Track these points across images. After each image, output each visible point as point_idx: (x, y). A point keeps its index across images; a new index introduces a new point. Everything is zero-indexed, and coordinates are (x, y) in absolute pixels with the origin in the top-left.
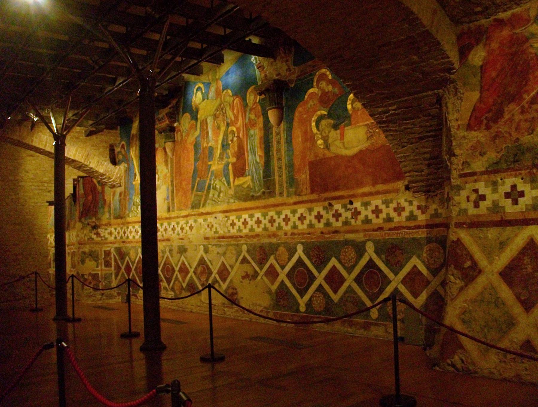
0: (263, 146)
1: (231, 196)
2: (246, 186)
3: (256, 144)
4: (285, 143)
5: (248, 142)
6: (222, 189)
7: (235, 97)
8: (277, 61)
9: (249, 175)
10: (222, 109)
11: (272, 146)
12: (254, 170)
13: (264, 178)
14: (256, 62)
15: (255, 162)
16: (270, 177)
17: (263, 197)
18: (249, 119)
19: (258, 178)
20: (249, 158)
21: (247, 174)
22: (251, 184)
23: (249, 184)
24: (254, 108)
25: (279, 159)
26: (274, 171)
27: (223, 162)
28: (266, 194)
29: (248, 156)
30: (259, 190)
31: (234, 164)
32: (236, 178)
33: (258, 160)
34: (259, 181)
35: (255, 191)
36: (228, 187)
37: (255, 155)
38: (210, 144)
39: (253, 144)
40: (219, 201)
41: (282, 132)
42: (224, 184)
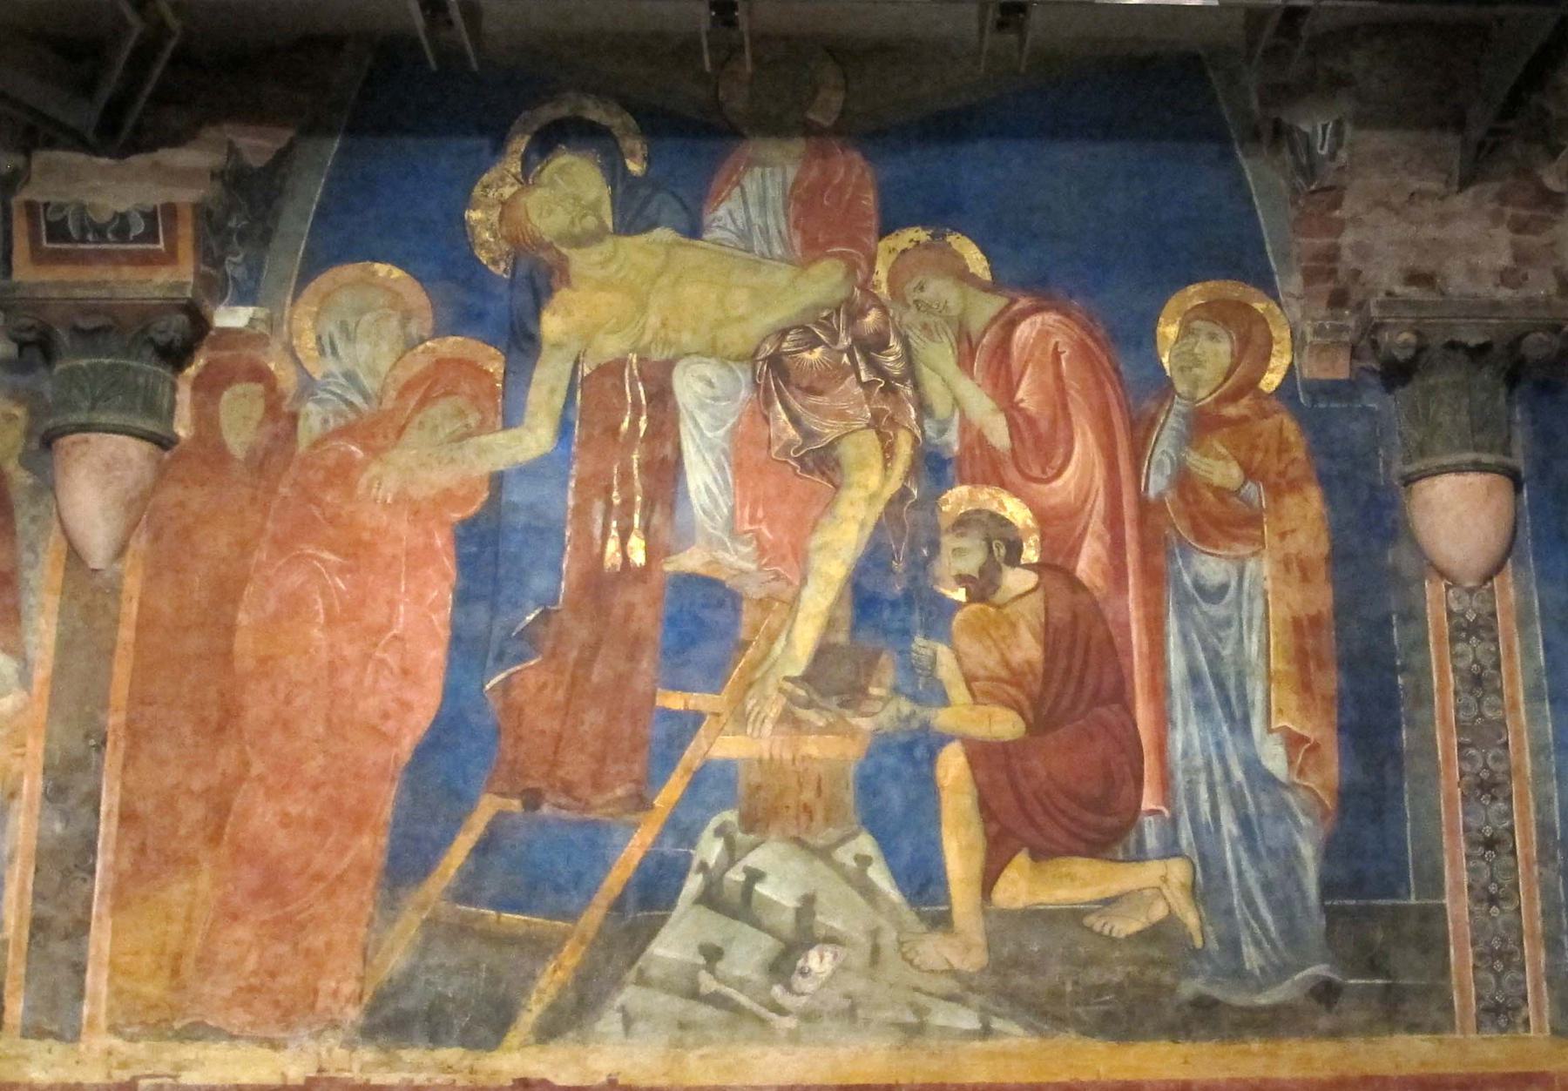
0: (1329, 681)
1: (949, 984)
2: (1125, 926)
3: (1253, 647)
4: (1534, 695)
5: (1173, 625)
6: (830, 919)
7: (1023, 303)
8: (1461, 202)
9: (1171, 850)
10: (872, 347)
11: (1422, 698)
12: (1229, 826)
13: (1328, 888)
14: (1333, 156)
15: (1238, 774)
16: (1394, 895)
17: (1324, 1022)
18: (1184, 480)
19: (1267, 888)
20: (1177, 739)
21: (1151, 842)
22: (1191, 919)
23: (1171, 919)
24: (1229, 422)
25: (1487, 787)
26: (1431, 851)
27: (865, 724)
28: (1343, 1003)
29: (1163, 721)
30: (1282, 972)
31: (982, 754)
32: (1022, 859)
33: (1275, 759)
34: (1282, 908)
35: (1238, 974)
36: (909, 916)
37: (1241, 724)
38: (691, 561)
39: (1227, 652)
40: (781, 1011)
41: (1505, 623)
42: (868, 891)
